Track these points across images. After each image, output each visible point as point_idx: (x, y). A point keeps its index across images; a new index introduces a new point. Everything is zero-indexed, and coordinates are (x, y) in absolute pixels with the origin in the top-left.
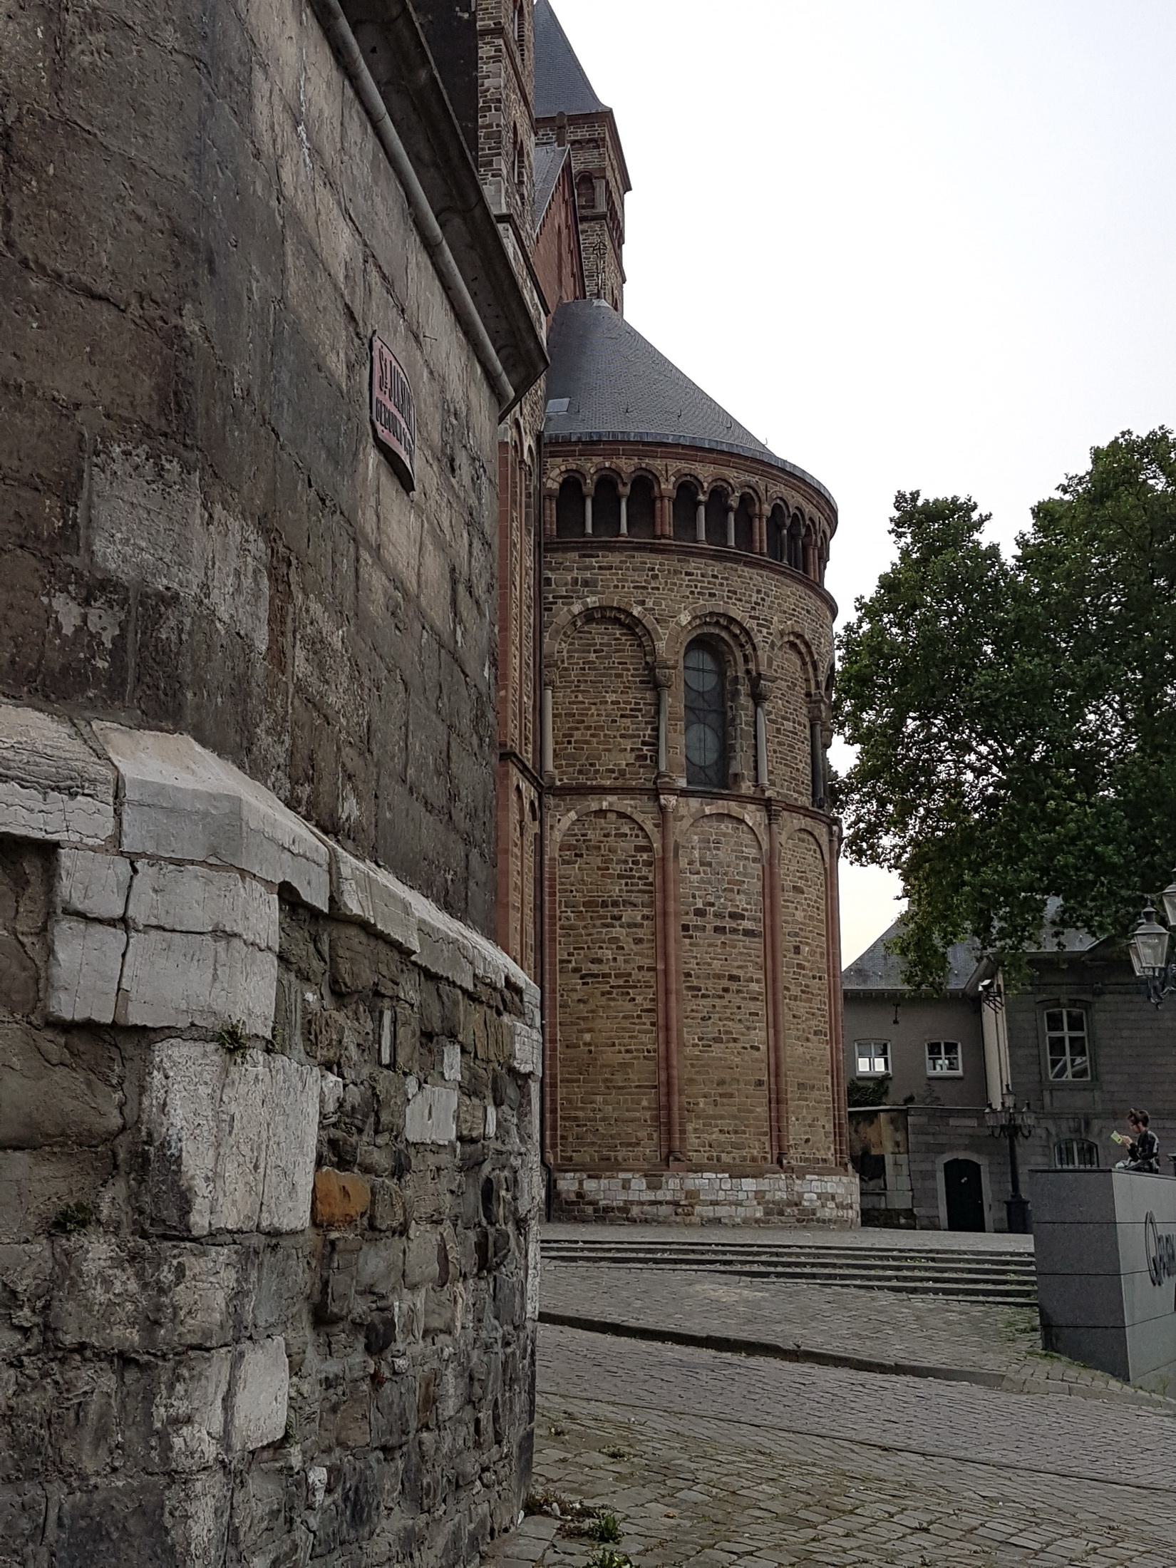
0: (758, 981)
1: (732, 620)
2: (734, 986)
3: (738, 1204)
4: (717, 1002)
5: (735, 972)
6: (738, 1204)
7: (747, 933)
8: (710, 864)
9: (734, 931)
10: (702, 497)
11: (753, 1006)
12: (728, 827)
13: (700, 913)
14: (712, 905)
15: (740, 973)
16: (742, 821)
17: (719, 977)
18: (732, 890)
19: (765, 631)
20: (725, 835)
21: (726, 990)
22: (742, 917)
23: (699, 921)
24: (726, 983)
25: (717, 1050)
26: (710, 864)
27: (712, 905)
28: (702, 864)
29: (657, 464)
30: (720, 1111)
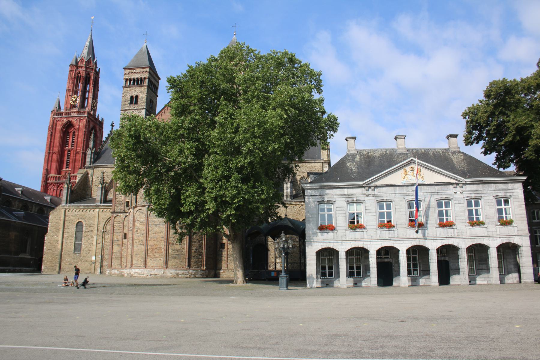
7: (131, 230)
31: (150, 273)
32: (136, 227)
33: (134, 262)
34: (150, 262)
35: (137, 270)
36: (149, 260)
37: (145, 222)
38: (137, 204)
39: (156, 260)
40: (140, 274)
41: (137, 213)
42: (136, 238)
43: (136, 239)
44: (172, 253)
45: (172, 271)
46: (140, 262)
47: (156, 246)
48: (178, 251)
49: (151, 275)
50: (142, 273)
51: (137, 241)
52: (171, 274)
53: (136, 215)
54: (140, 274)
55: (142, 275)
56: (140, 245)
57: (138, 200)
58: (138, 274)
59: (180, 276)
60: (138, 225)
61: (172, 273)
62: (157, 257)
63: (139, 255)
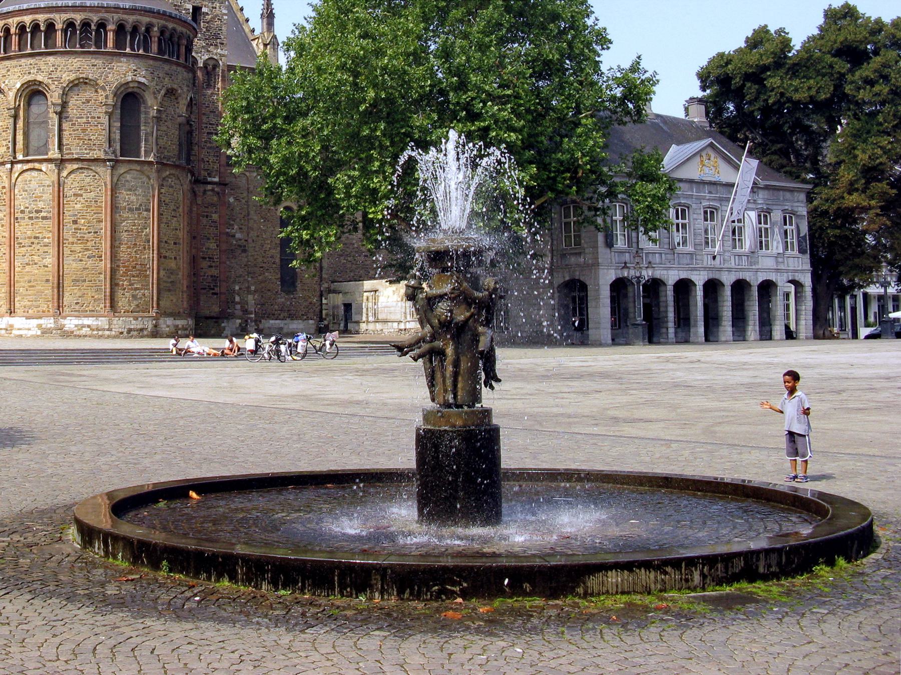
0: (48, 238)
1: (40, 82)
2: (36, 241)
3: (29, 329)
4: (29, 249)
5: (37, 235)
6: (29, 329)
7: (44, 218)
8: (26, 191)
9: (37, 218)
10: (28, 30)
11: (46, 249)
12: (34, 174)
13: (22, 212)
14: (28, 208)
15: (40, 235)
16: (41, 170)
17: (29, 238)
18: (36, 201)
19: (56, 83)
20: (34, 177)
21: (33, 243)
22: (41, 211)
23: (22, 215)
24: (33, 240)
25: (28, 268)
26: (26, 191)
27: (28, 208)
28: (24, 191)
29: (10, 20)
30: (29, 292)
31: (128, 327)
32: (70, 213)
33: (67, 299)
34: (123, 302)
35: (87, 321)
36: (119, 293)
37: (105, 199)
38: (65, 151)
39: (134, 297)
40: (98, 329)
41: (73, 176)
42: (71, 240)
43: (73, 243)
44: (165, 279)
45: (170, 321)
46: (90, 299)
47: (133, 261)
48: (172, 273)
49: (130, 331)
50: (107, 327)
51: (78, 248)
52: (168, 329)
53: (69, 181)
54: (98, 329)
55: (107, 333)
56: (88, 257)
57: (65, 142)
58: (93, 330)
59: (180, 332)
60: (78, 206)
61: (168, 326)
62: (136, 289)
63: (87, 283)
